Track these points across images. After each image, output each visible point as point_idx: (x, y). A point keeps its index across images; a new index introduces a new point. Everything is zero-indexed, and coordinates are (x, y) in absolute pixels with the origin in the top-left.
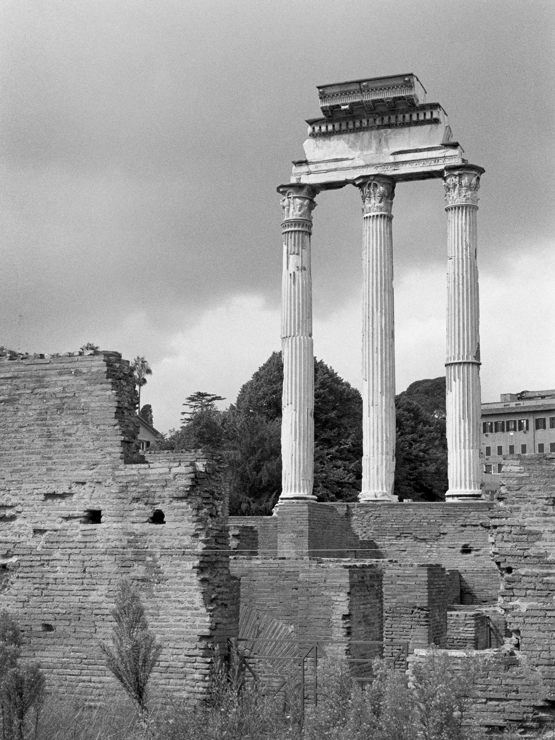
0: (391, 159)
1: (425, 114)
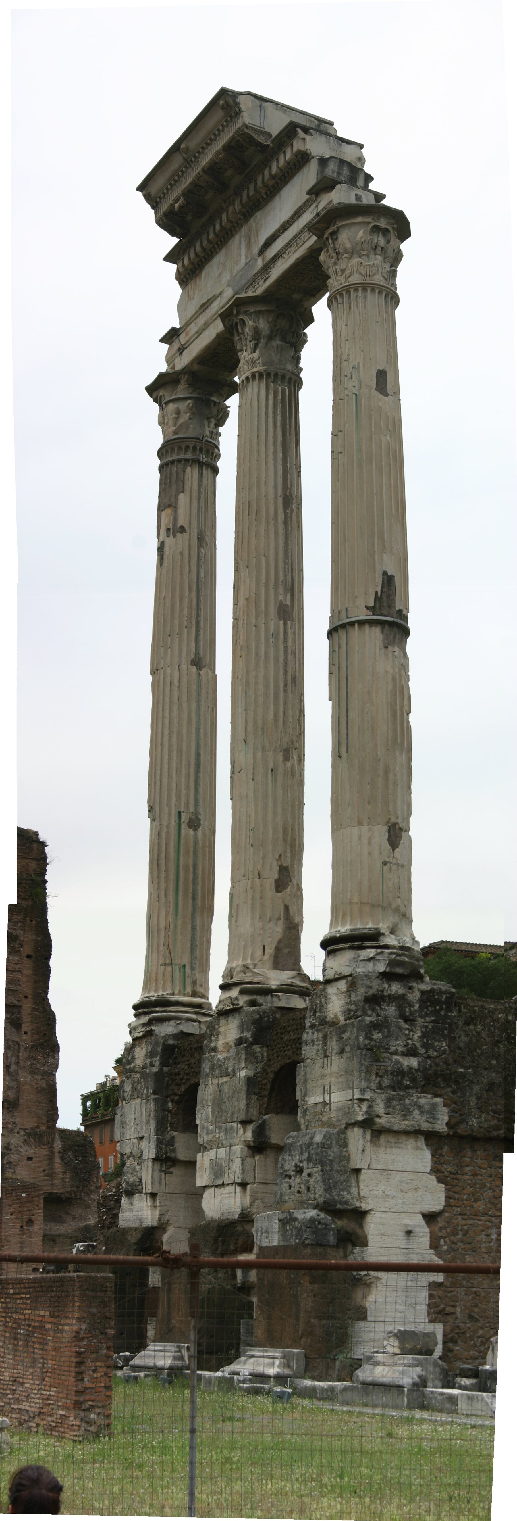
0: (260, 263)
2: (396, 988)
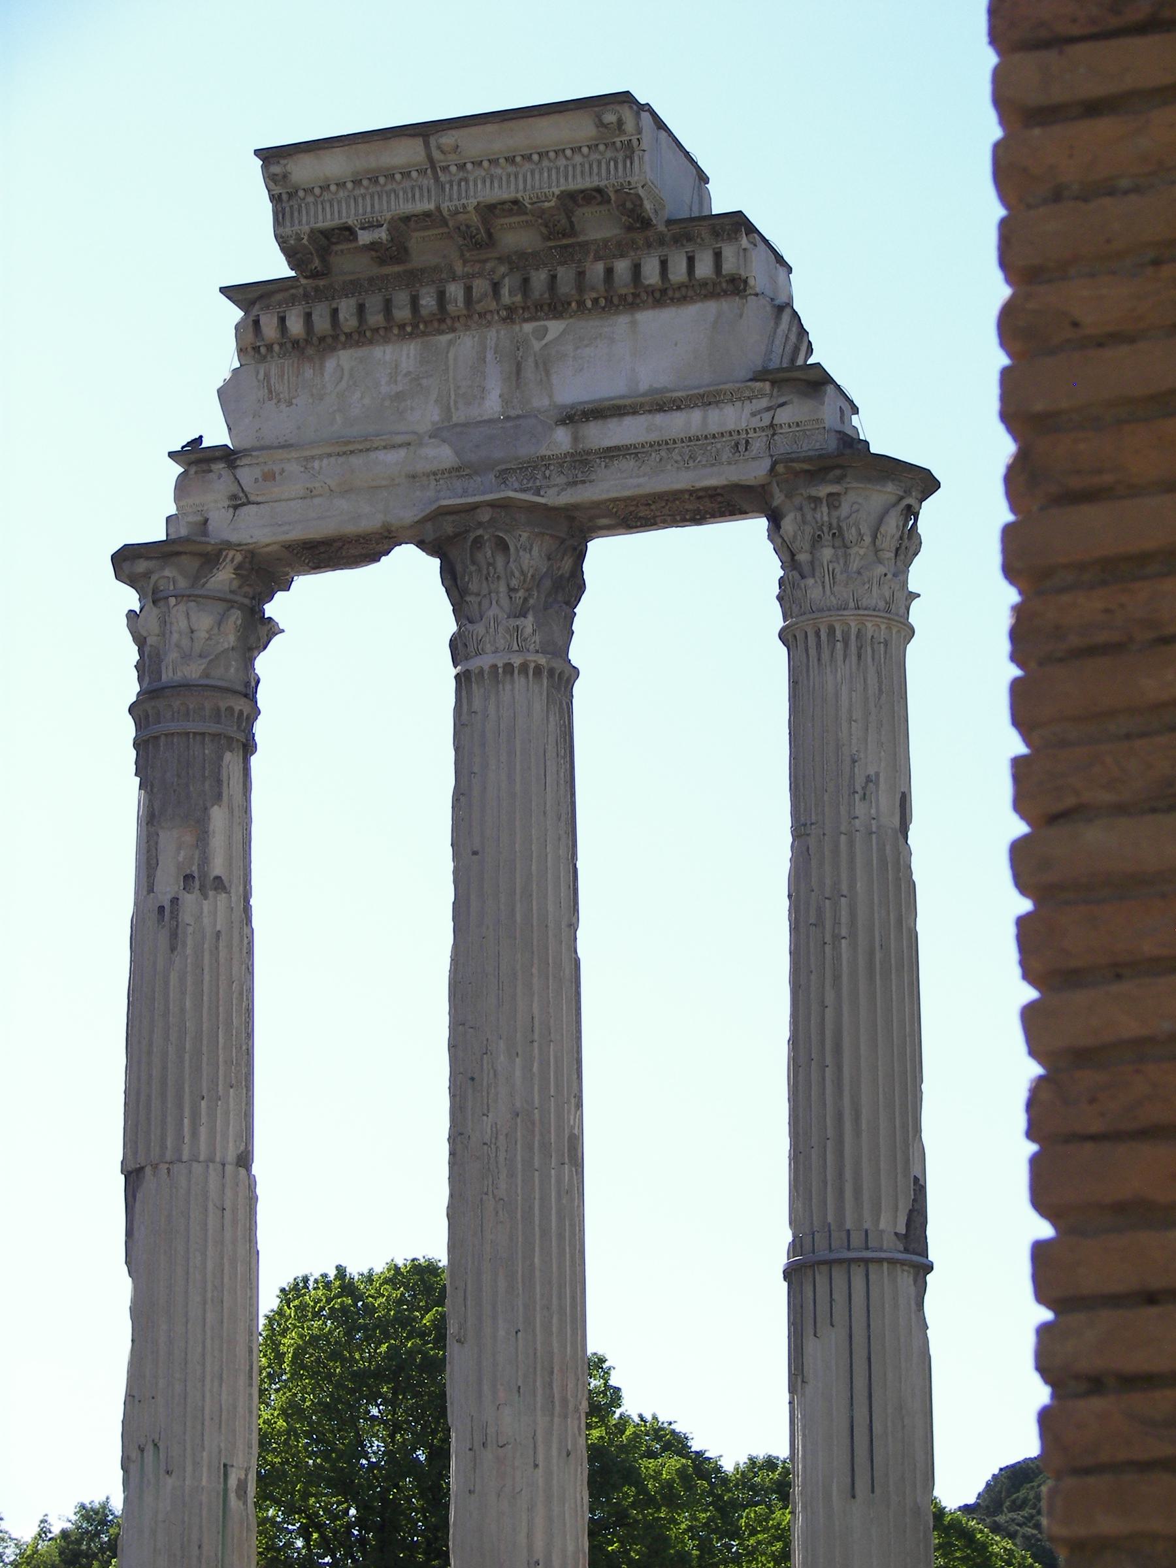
0: (562, 439)
1: (691, 261)
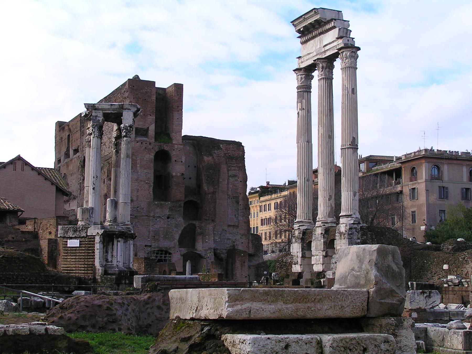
0: (323, 50)
2: (355, 226)
